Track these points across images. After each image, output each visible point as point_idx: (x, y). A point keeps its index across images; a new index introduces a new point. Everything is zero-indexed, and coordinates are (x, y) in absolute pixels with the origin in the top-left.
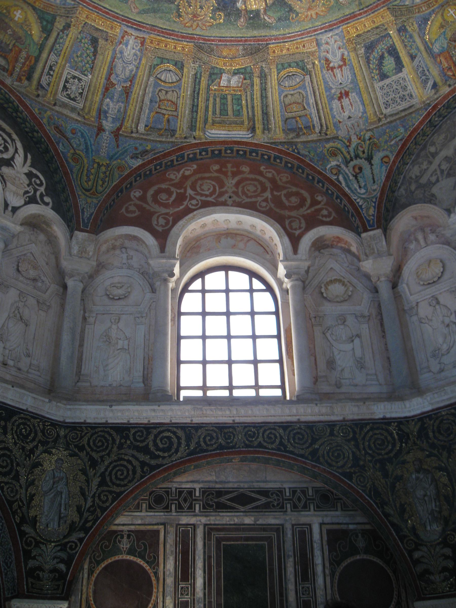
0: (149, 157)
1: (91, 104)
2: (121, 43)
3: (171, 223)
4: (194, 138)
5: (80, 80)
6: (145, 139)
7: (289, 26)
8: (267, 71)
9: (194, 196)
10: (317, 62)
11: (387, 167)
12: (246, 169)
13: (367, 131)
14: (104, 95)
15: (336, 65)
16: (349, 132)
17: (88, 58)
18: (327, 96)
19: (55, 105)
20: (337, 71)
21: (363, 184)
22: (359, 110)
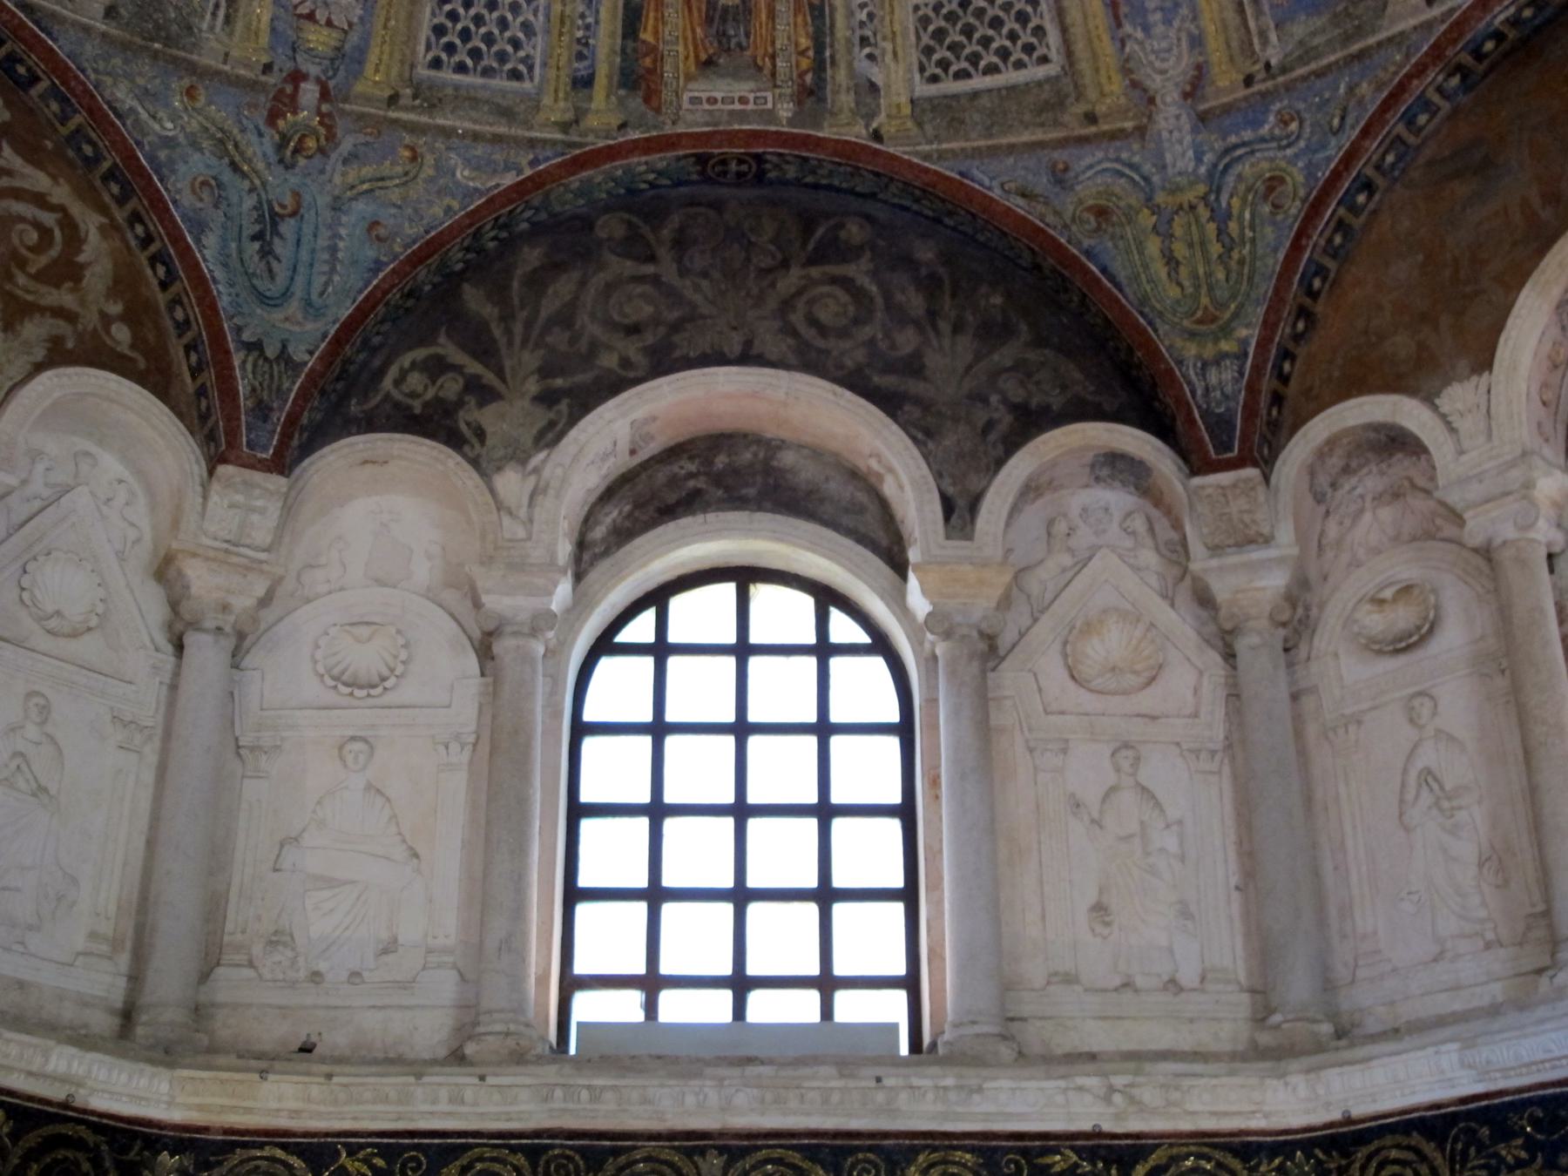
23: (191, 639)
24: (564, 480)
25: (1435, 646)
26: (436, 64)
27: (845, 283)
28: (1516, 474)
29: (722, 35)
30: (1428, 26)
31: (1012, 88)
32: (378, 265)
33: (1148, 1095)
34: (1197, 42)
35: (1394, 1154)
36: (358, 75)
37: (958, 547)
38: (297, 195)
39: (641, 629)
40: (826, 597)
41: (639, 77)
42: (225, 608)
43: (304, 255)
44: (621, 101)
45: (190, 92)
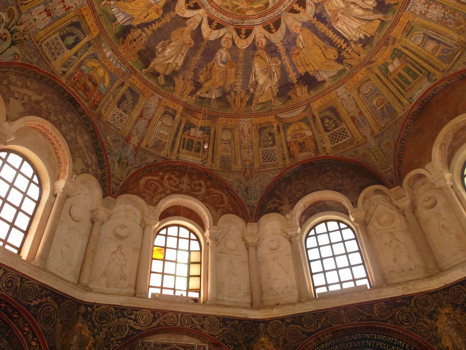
11: (13, 60)
13: (29, 35)
15: (66, 3)
16: (26, 21)
20: (62, 5)
22: (41, 26)
23: (249, 248)
24: (296, 214)
25: (437, 206)
26: (264, 162)
27: (329, 176)
28: (441, 175)
30: (405, 114)
31: (345, 142)
32: (262, 191)
33: (411, 287)
34: (370, 127)
35: (456, 289)
37: (356, 209)
38: (250, 184)
39: (312, 233)
40: (339, 222)
41: (291, 156)
42: (253, 243)
45: (233, 175)
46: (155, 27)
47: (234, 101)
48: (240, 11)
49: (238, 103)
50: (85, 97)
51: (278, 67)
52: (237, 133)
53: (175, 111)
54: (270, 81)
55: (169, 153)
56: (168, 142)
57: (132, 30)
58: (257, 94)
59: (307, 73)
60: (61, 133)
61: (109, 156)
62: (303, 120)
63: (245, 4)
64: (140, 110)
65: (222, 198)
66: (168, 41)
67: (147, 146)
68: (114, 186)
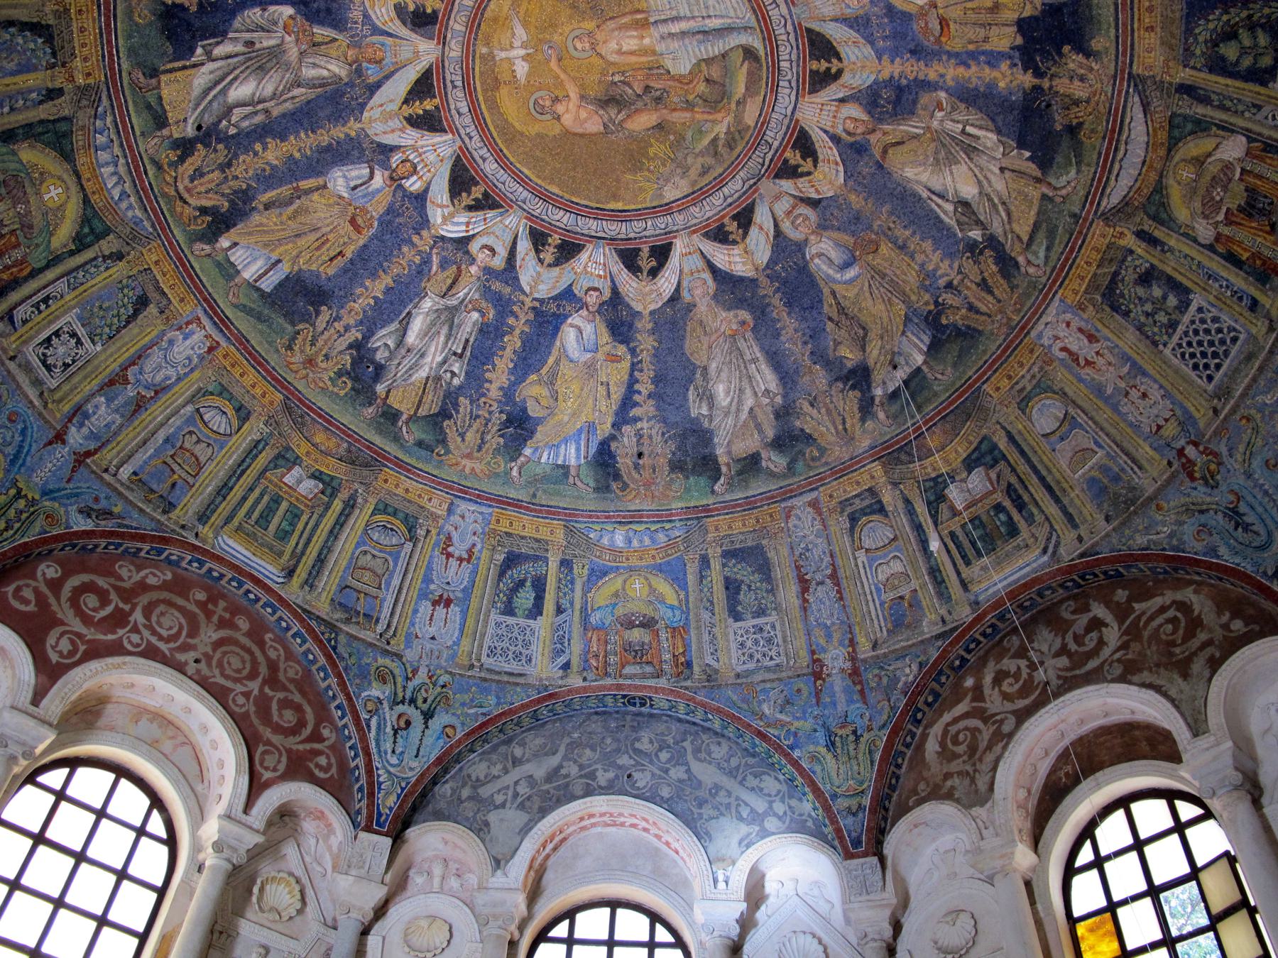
0: (108, 525)
1: (72, 390)
2: (180, 328)
3: (78, 656)
4: (197, 534)
5: (79, 342)
6: (120, 494)
7: (428, 461)
8: (360, 500)
9: (141, 628)
10: (434, 532)
12: (244, 624)
13: (447, 672)
14: (102, 389)
15: (457, 554)
17: (115, 320)
18: (420, 589)
19: (12, 358)
20: (453, 563)
21: (399, 750)
26: (1210, 378)
29: (1262, 212)
36: (1195, 423)
43: (1260, 510)
44: (1271, 289)
46: (645, 387)
47: (971, 308)
48: (733, 139)
49: (986, 303)
50: (648, 669)
51: (954, 109)
52: (1061, 377)
53: (870, 490)
54: (983, 160)
55: (943, 612)
56: (921, 582)
57: (613, 445)
58: (997, 228)
59: (1023, 25)
60: (635, 797)
61: (796, 754)
62: (1176, 133)
63: (719, 116)
64: (792, 574)
65: (1184, 607)
66: (698, 376)
67: (875, 646)
68: (850, 820)
